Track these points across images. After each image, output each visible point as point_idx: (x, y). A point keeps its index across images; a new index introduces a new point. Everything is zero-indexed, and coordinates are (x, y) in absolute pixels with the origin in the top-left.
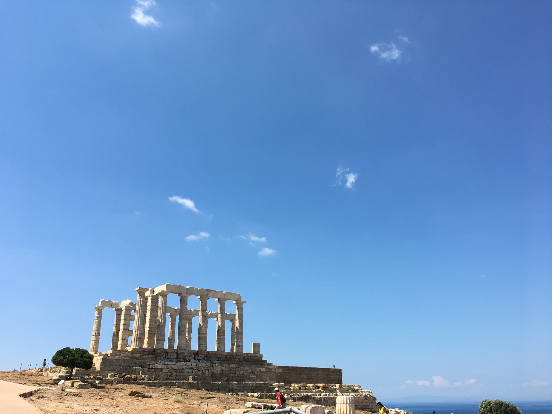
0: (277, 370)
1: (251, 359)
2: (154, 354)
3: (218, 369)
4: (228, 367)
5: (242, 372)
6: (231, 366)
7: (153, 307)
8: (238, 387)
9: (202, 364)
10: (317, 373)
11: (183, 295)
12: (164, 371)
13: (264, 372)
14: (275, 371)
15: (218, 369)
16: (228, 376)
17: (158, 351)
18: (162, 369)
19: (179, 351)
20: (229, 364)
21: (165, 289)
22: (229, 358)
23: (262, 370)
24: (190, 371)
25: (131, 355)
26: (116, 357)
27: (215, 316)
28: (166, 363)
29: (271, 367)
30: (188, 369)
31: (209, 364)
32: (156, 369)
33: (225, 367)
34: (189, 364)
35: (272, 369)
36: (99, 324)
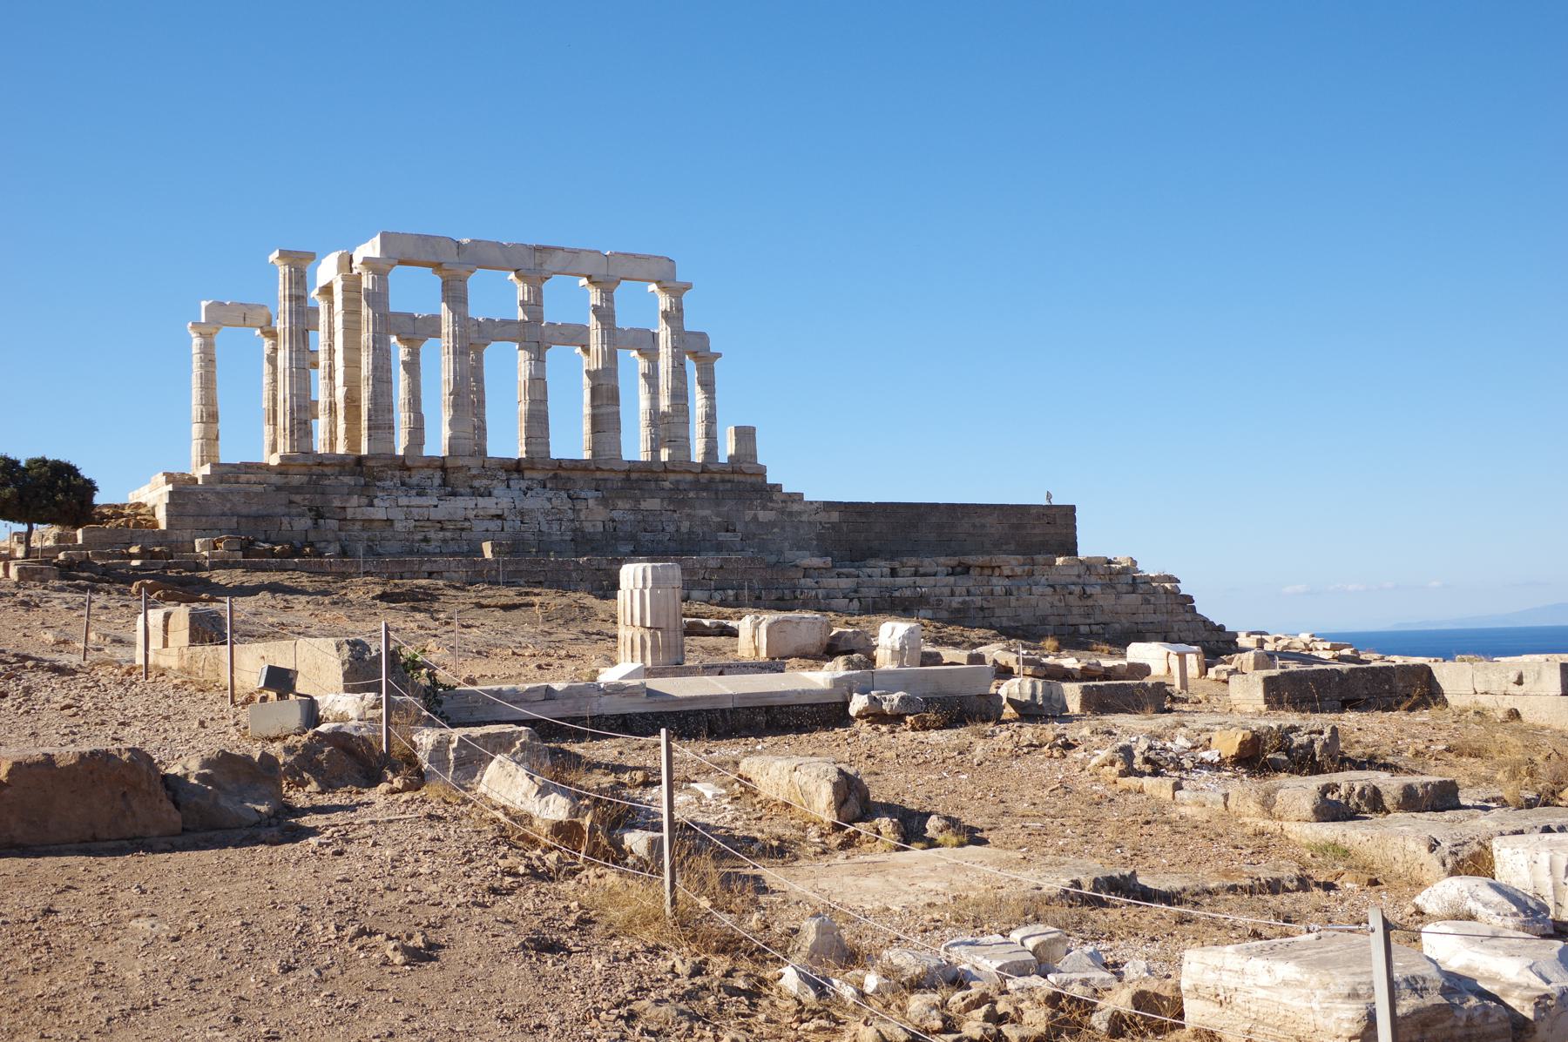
0: (822, 517)
1: (723, 481)
2: (361, 474)
4: (635, 510)
5: (685, 526)
6: (644, 505)
7: (354, 318)
10: (977, 521)
11: (453, 265)
12: (399, 526)
13: (773, 524)
14: (813, 518)
15: (594, 516)
16: (632, 538)
18: (390, 521)
19: (449, 464)
21: (376, 254)
23: (764, 516)
24: (494, 525)
25: (275, 479)
26: (219, 487)
27: (577, 336)
29: (796, 507)
31: (561, 501)
33: (622, 511)
35: (800, 513)
36: (208, 383)
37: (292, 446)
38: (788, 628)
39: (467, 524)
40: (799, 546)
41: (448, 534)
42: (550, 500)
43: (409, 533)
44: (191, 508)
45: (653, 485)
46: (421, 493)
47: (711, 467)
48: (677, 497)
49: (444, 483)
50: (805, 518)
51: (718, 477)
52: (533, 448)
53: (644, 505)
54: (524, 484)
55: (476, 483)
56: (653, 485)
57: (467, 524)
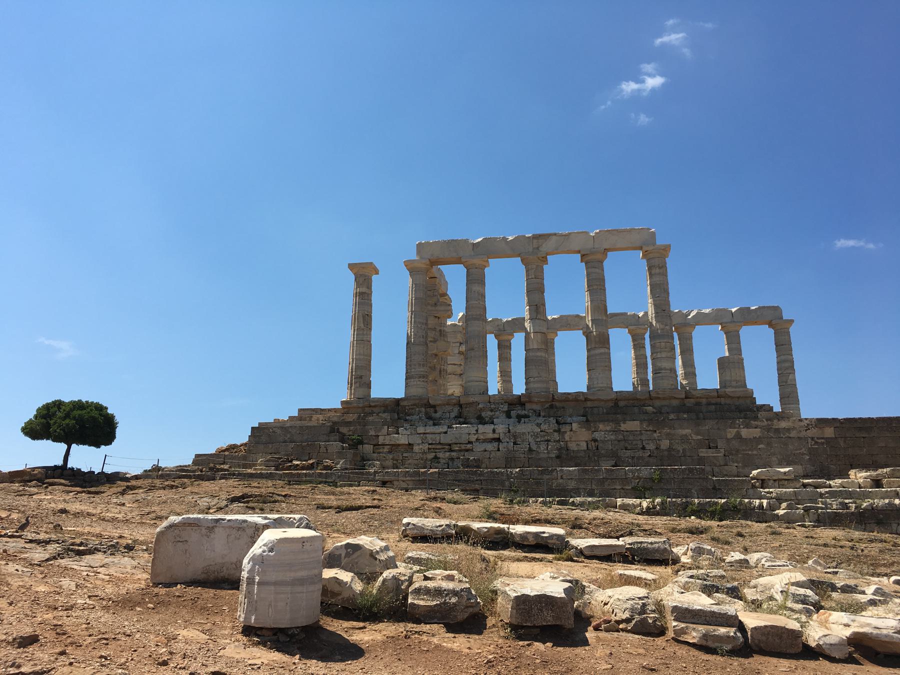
1: (709, 404)
3: (578, 437)
5: (665, 444)
6: (623, 427)
8: (580, 480)
9: (526, 428)
12: (416, 448)
13: (758, 440)
14: (803, 434)
15: (578, 437)
17: (405, 403)
18: (410, 445)
20: (617, 423)
22: (621, 406)
23: (745, 433)
24: (489, 447)
28: (421, 430)
29: (783, 424)
30: (485, 441)
31: (549, 426)
32: (399, 445)
35: (788, 430)
37: (351, 394)
38: (194, 536)
39: (469, 446)
41: (454, 454)
42: (539, 425)
43: (424, 453)
44: (264, 439)
45: (636, 410)
47: (694, 393)
50: (793, 434)
51: (704, 401)
52: (532, 385)
53: (623, 427)
56: (636, 410)
57: (469, 446)
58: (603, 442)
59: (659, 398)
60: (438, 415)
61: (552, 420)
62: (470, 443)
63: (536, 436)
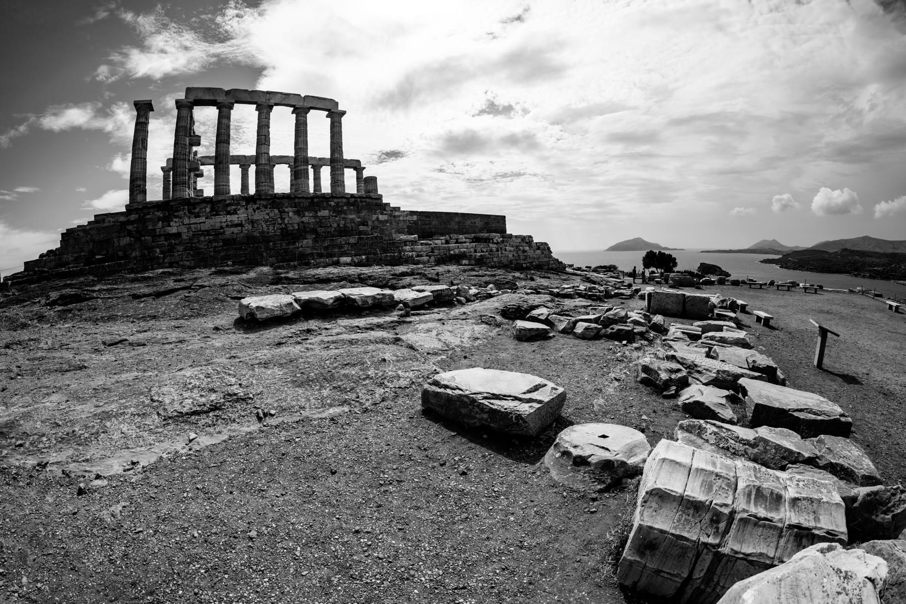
4: (316, 217)
6: (319, 214)
13: (386, 221)
17: (172, 204)
18: (179, 235)
23: (381, 217)
24: (236, 230)
28: (186, 221)
29: (397, 214)
33: (308, 217)
34: (234, 218)
40: (400, 232)
42: (268, 214)
43: (190, 239)
46: (197, 216)
48: (337, 211)
49: (212, 210)
50: (401, 218)
53: (319, 214)
54: (255, 207)
55: (229, 209)
58: (308, 223)
59: (336, 198)
60: (197, 210)
61: (276, 211)
62: (222, 228)
63: (266, 221)
